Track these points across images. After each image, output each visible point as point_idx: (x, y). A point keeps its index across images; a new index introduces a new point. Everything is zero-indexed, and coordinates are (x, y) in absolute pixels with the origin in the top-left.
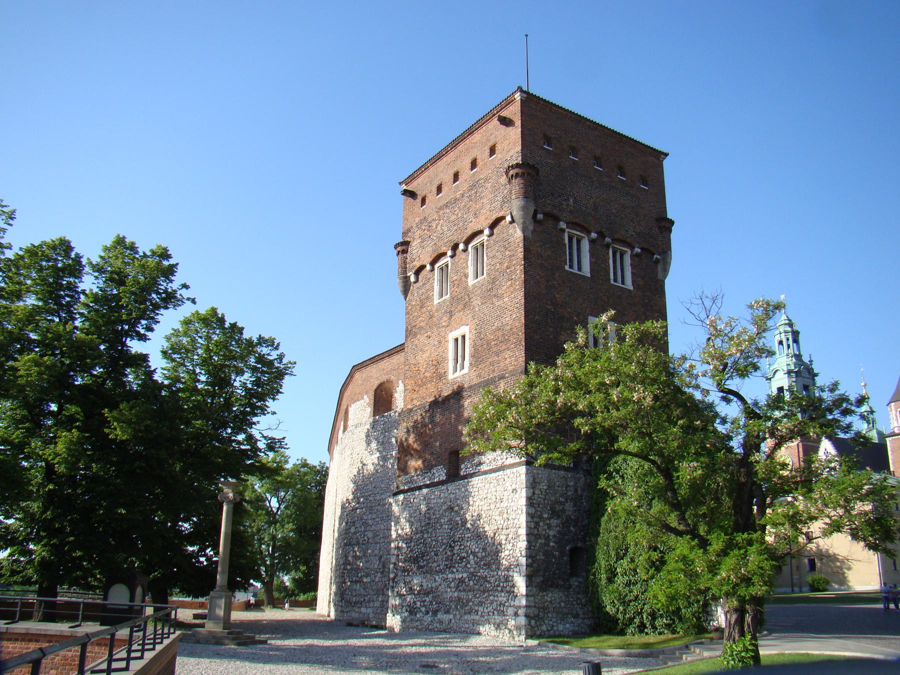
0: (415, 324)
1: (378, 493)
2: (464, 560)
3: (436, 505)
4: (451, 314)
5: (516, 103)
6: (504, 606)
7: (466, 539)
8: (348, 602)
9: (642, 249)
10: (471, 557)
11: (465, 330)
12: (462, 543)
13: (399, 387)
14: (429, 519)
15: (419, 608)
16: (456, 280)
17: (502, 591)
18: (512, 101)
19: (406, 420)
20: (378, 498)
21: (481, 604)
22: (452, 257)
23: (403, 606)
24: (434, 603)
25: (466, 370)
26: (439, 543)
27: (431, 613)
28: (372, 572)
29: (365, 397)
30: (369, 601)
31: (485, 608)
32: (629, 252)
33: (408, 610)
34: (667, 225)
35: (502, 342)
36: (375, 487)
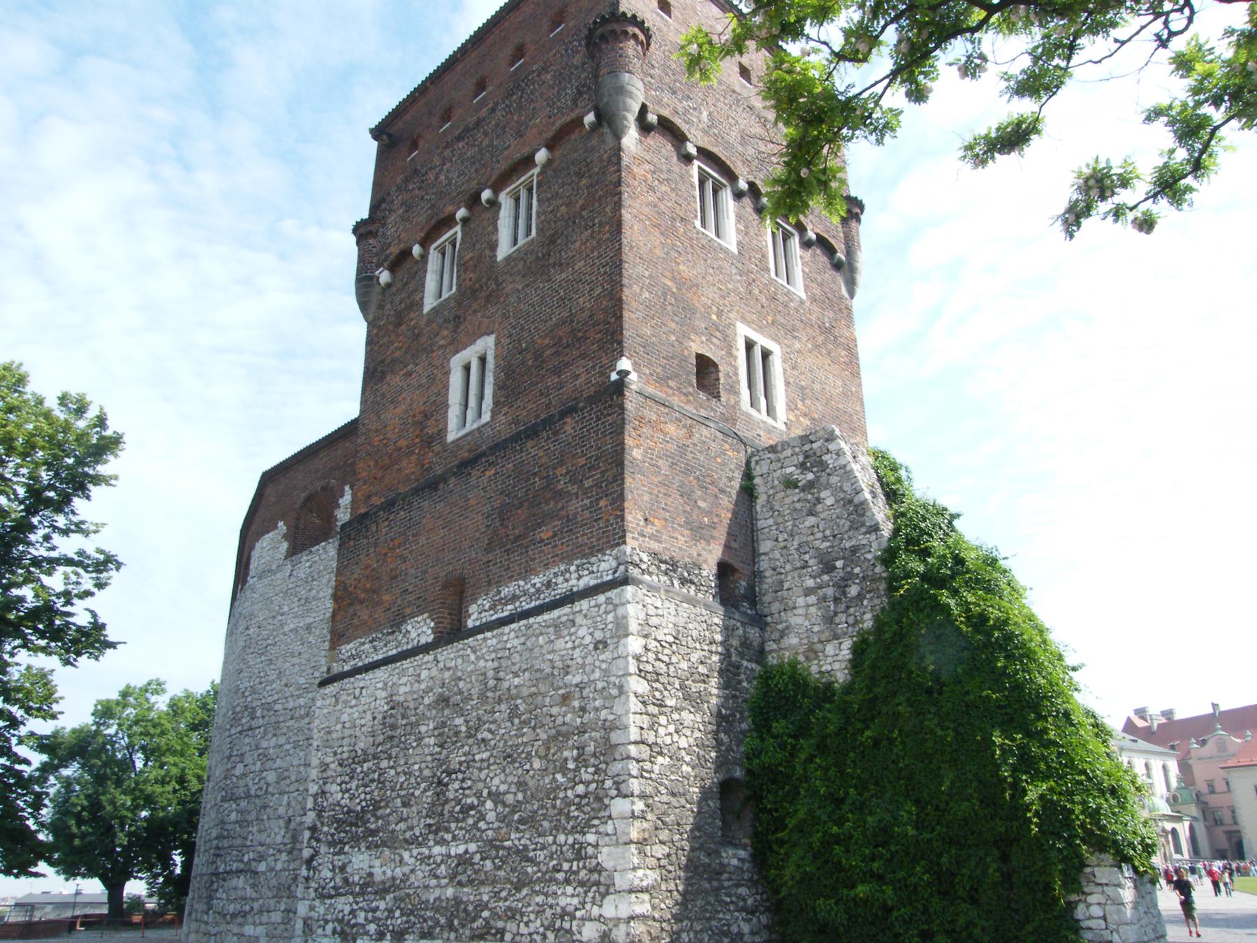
1: (292, 696)
2: (472, 813)
3: (410, 698)
4: (458, 320)
6: (573, 917)
7: (478, 765)
8: (219, 913)
9: (817, 235)
10: (489, 804)
11: (487, 344)
12: (468, 774)
13: (345, 497)
14: (393, 727)
15: (363, 926)
16: (472, 259)
17: (567, 881)
19: (353, 536)
20: (291, 705)
21: (512, 914)
23: (326, 922)
24: (397, 914)
25: (486, 417)
26: (412, 780)
27: (388, 936)
28: (271, 851)
29: (281, 524)
30: (261, 912)
31: (522, 925)
33: (339, 929)
34: (857, 210)
35: (568, 346)
36: (286, 685)
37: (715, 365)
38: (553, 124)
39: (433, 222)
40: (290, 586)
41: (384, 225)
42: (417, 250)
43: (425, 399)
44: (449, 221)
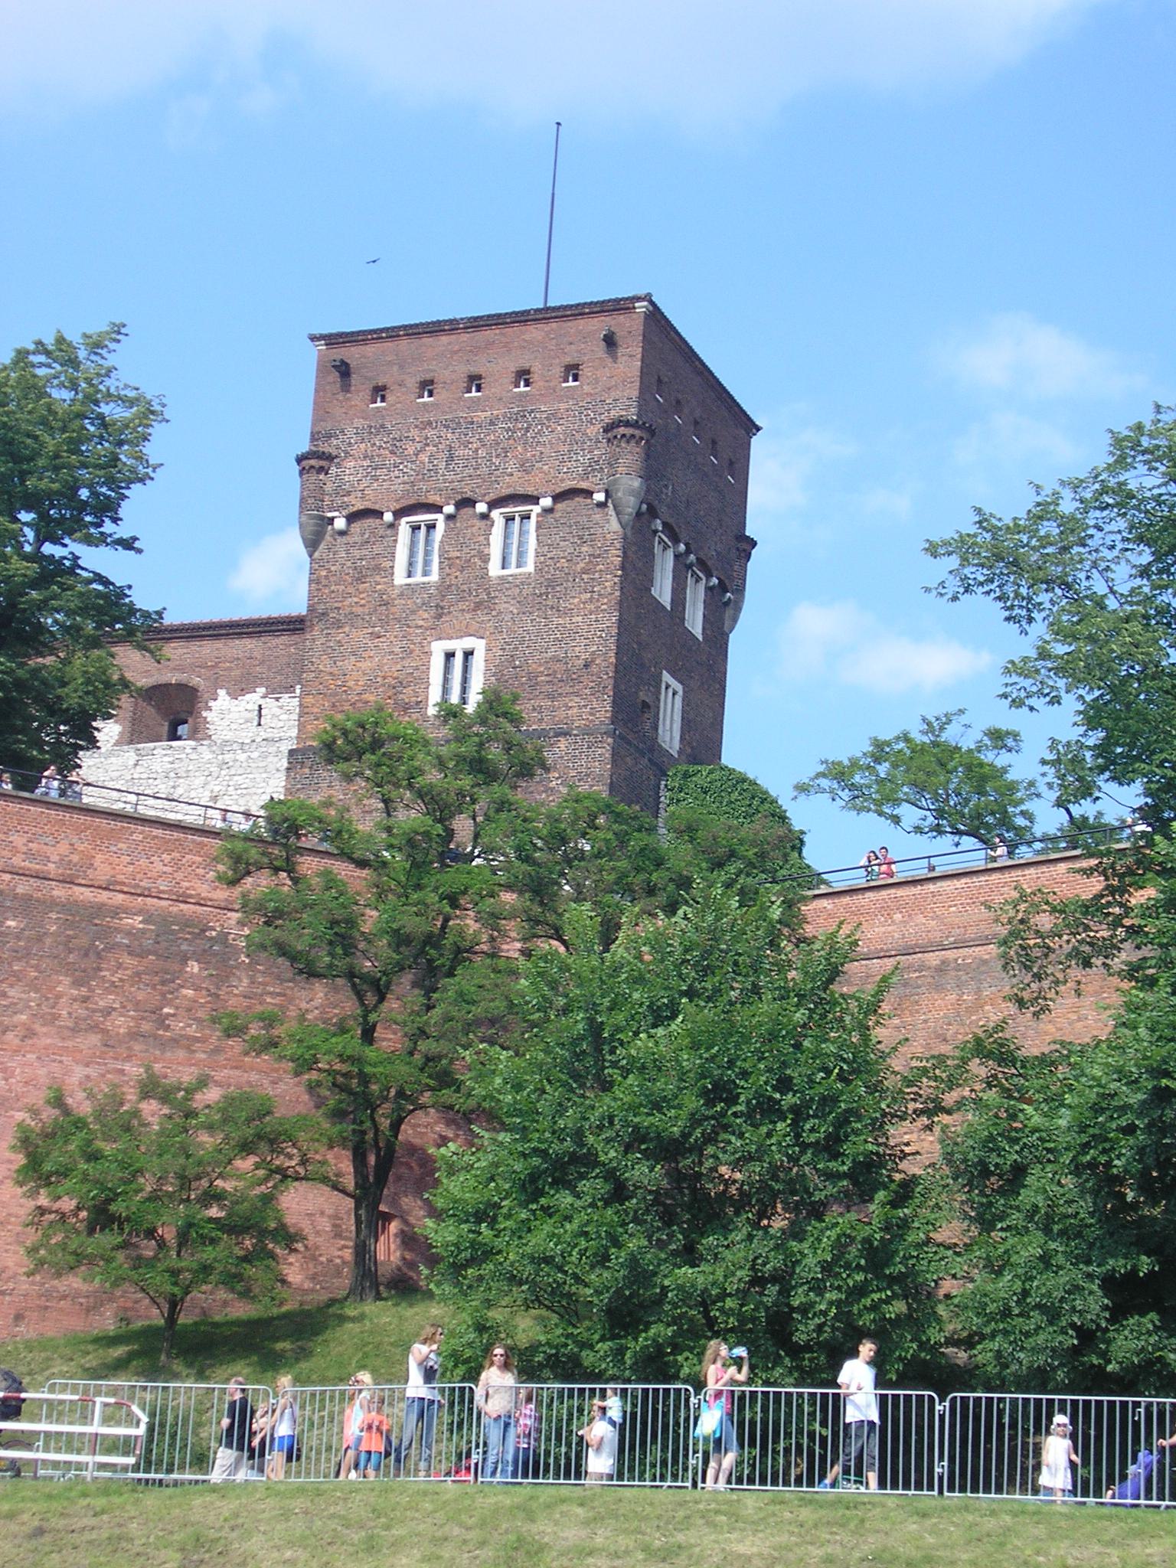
0: (336, 605)
5: (634, 316)
11: (479, 645)
18: (628, 308)
22: (450, 518)
32: (704, 581)
37: (649, 707)
38: (562, 480)
39: (412, 502)
40: (136, 776)
41: (339, 465)
42: (388, 517)
43: (399, 667)
44: (438, 509)
